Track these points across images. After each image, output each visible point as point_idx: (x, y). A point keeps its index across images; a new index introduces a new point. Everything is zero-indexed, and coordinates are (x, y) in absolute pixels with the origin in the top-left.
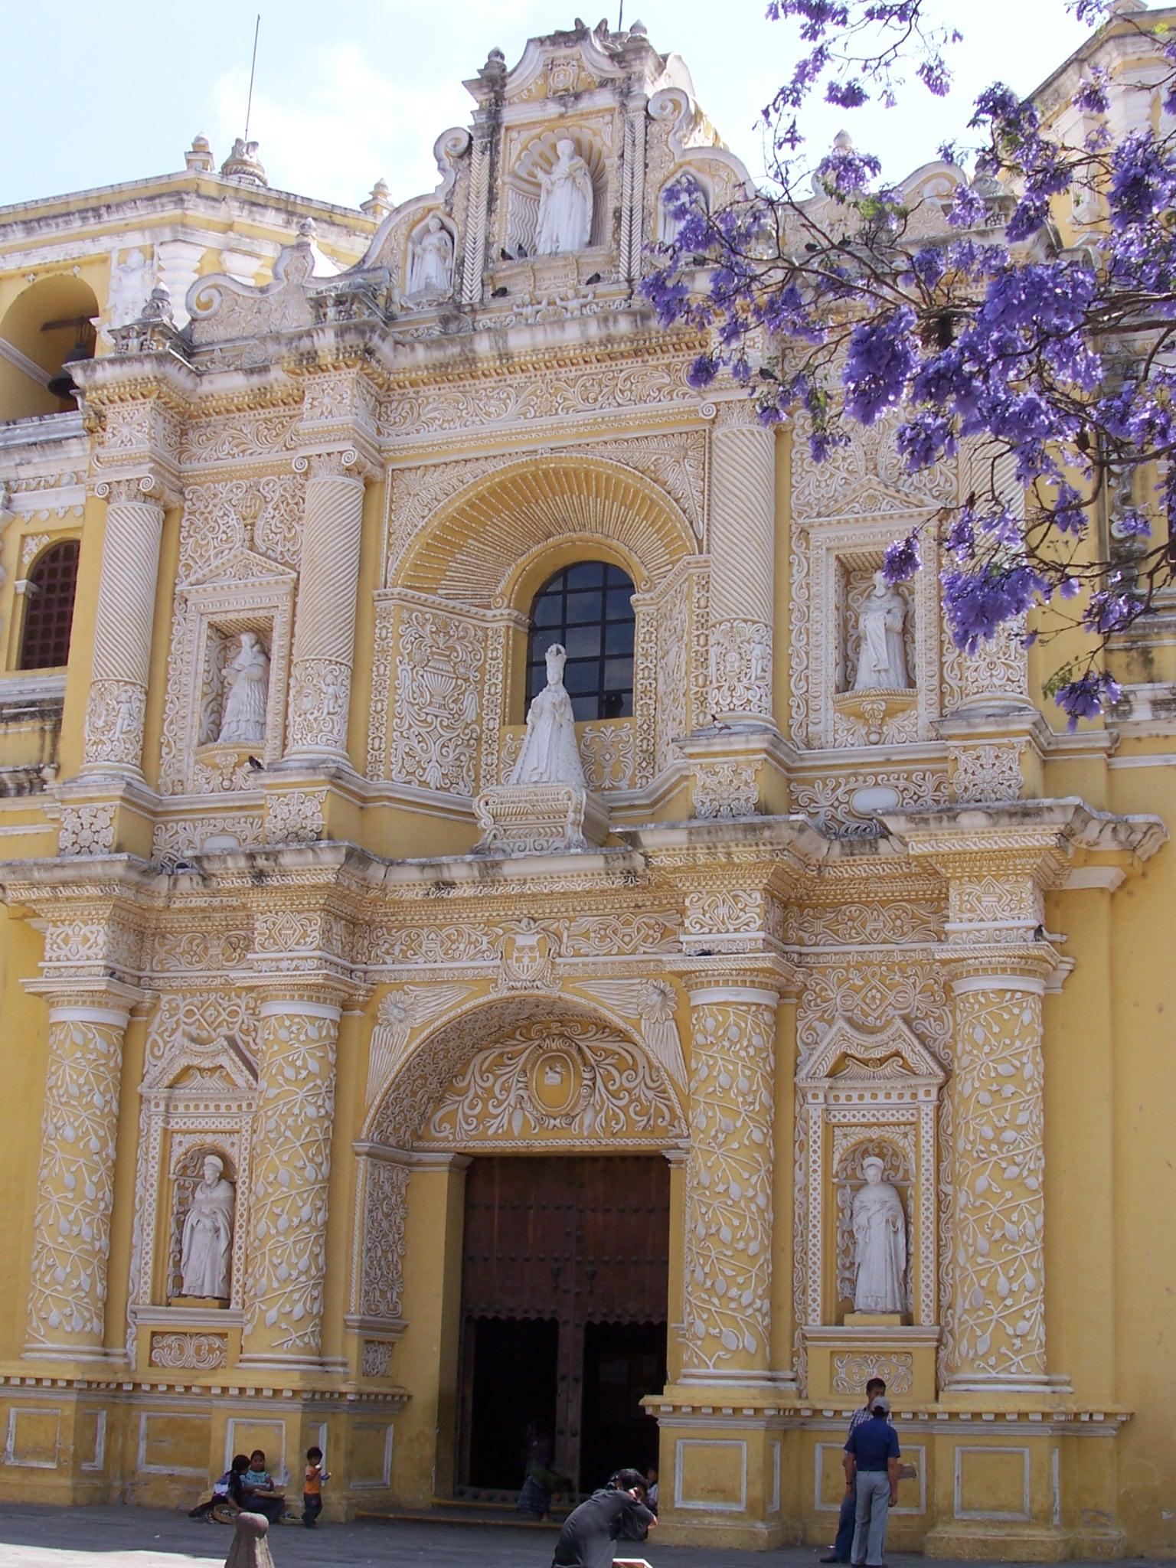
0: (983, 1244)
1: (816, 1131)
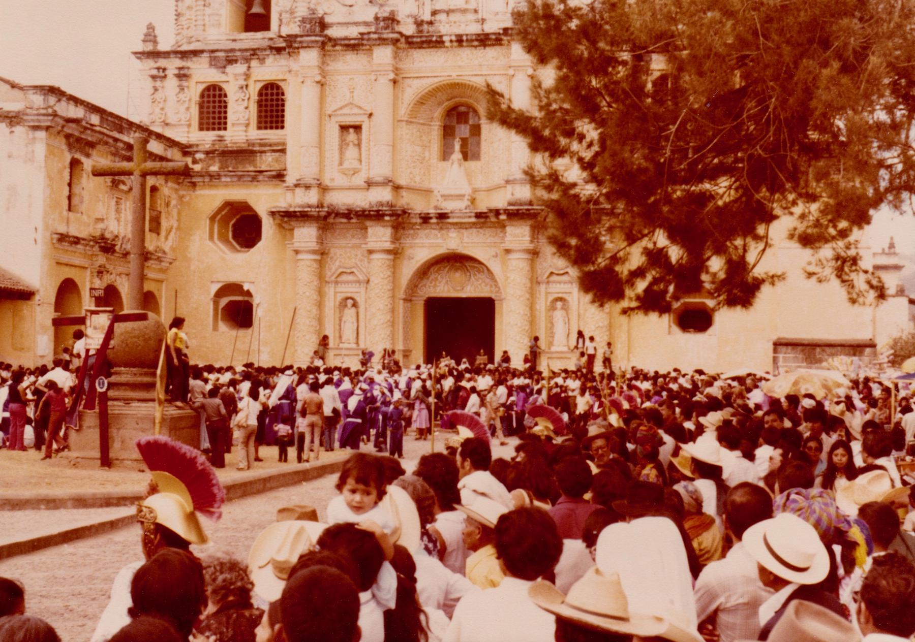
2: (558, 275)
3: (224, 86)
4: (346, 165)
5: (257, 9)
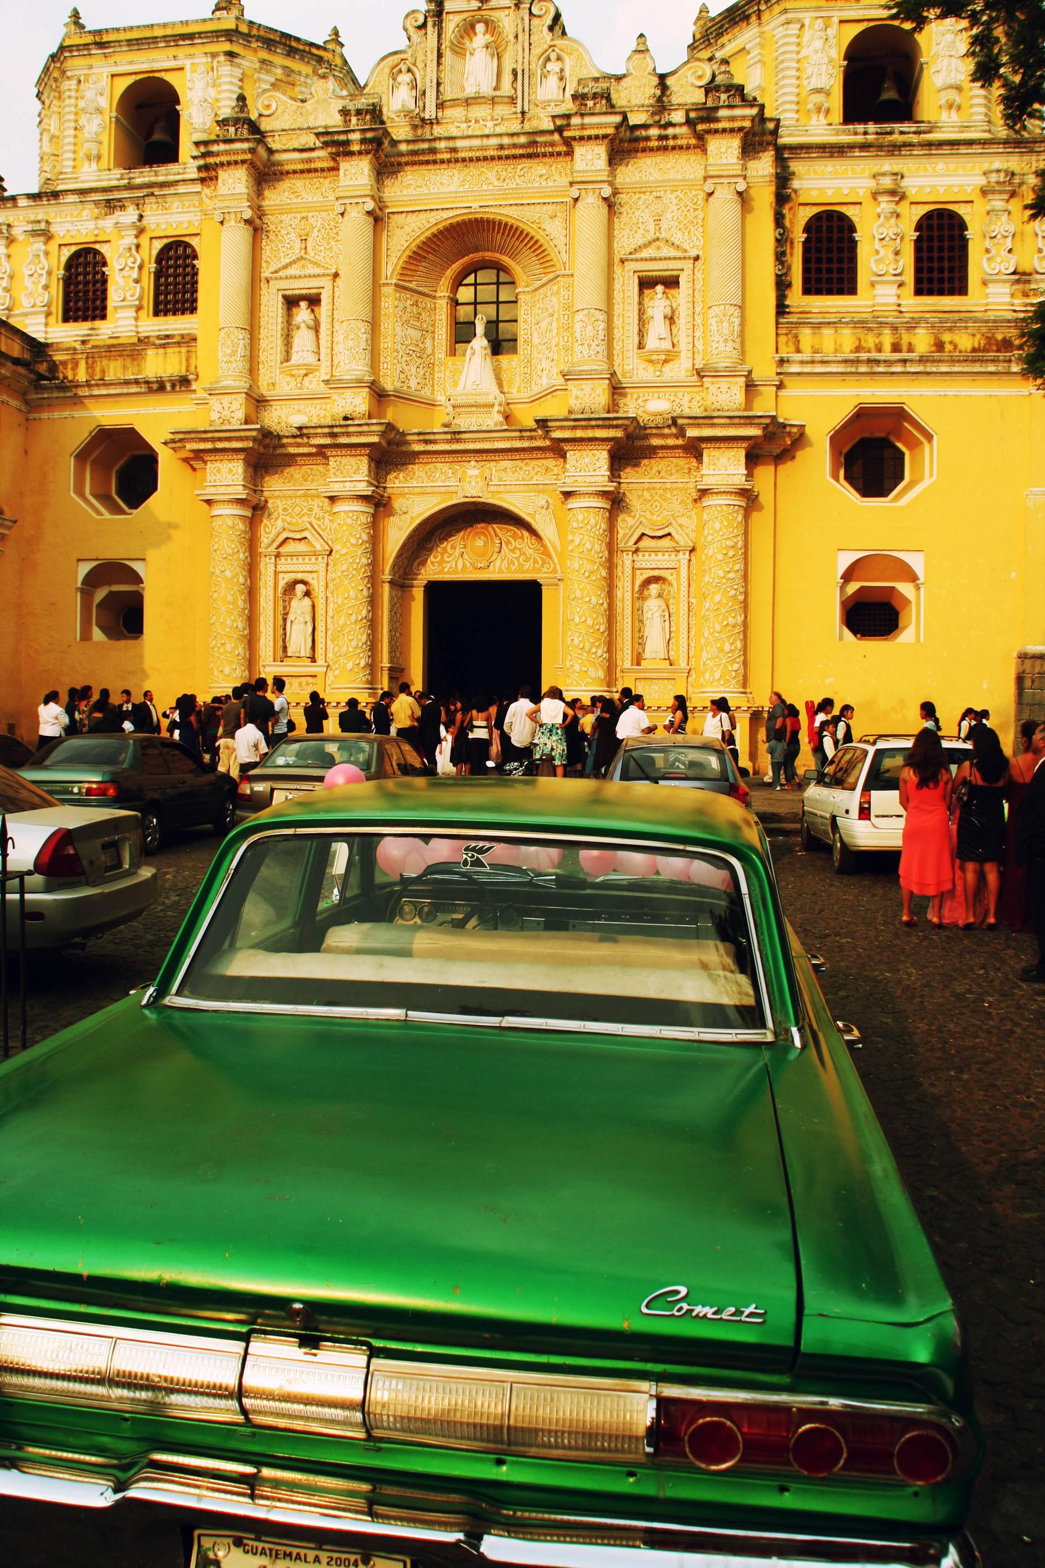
0: (718, 627)
1: (628, 570)
2: (653, 537)
3: (103, 249)
4: (295, 359)
5: (157, 136)
